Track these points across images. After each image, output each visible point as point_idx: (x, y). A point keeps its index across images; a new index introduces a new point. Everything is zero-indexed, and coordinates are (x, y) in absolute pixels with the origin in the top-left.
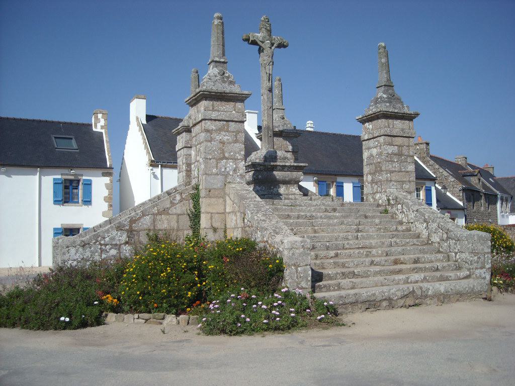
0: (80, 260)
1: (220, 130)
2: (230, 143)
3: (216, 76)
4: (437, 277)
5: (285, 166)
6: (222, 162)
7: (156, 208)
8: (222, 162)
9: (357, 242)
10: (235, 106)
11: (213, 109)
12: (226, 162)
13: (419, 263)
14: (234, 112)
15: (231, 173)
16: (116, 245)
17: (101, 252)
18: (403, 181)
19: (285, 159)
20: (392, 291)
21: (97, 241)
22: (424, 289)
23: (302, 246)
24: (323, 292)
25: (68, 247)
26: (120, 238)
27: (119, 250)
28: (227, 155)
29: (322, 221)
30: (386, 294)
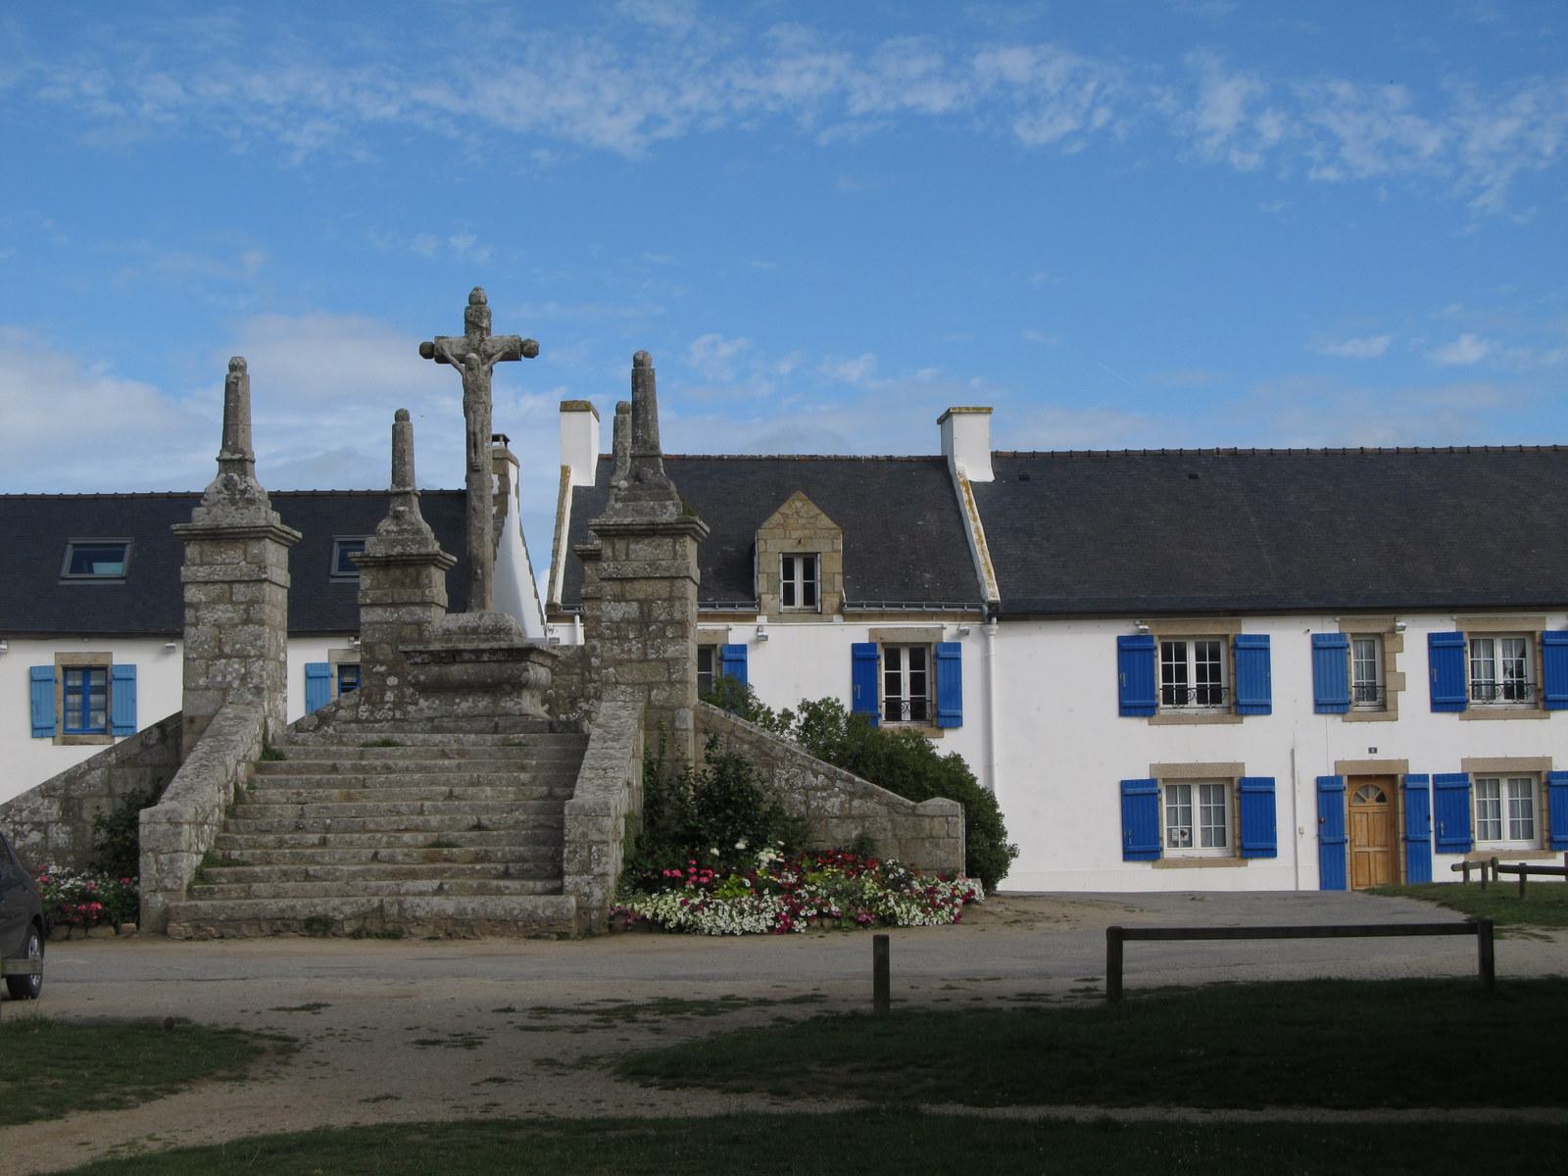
1: (213, 603)
2: (235, 626)
3: (219, 492)
4: (471, 886)
5: (483, 651)
7: (113, 755)
9: (421, 818)
10: (245, 552)
11: (201, 561)
12: (227, 664)
13: (489, 861)
14: (243, 563)
16: (40, 824)
17: (15, 835)
18: (652, 683)
19: (498, 633)
20: (331, 904)
21: (7, 816)
23: (169, 819)
24: (214, 899)
26: (49, 811)
27: (46, 833)
28: (227, 649)
29: (387, 778)
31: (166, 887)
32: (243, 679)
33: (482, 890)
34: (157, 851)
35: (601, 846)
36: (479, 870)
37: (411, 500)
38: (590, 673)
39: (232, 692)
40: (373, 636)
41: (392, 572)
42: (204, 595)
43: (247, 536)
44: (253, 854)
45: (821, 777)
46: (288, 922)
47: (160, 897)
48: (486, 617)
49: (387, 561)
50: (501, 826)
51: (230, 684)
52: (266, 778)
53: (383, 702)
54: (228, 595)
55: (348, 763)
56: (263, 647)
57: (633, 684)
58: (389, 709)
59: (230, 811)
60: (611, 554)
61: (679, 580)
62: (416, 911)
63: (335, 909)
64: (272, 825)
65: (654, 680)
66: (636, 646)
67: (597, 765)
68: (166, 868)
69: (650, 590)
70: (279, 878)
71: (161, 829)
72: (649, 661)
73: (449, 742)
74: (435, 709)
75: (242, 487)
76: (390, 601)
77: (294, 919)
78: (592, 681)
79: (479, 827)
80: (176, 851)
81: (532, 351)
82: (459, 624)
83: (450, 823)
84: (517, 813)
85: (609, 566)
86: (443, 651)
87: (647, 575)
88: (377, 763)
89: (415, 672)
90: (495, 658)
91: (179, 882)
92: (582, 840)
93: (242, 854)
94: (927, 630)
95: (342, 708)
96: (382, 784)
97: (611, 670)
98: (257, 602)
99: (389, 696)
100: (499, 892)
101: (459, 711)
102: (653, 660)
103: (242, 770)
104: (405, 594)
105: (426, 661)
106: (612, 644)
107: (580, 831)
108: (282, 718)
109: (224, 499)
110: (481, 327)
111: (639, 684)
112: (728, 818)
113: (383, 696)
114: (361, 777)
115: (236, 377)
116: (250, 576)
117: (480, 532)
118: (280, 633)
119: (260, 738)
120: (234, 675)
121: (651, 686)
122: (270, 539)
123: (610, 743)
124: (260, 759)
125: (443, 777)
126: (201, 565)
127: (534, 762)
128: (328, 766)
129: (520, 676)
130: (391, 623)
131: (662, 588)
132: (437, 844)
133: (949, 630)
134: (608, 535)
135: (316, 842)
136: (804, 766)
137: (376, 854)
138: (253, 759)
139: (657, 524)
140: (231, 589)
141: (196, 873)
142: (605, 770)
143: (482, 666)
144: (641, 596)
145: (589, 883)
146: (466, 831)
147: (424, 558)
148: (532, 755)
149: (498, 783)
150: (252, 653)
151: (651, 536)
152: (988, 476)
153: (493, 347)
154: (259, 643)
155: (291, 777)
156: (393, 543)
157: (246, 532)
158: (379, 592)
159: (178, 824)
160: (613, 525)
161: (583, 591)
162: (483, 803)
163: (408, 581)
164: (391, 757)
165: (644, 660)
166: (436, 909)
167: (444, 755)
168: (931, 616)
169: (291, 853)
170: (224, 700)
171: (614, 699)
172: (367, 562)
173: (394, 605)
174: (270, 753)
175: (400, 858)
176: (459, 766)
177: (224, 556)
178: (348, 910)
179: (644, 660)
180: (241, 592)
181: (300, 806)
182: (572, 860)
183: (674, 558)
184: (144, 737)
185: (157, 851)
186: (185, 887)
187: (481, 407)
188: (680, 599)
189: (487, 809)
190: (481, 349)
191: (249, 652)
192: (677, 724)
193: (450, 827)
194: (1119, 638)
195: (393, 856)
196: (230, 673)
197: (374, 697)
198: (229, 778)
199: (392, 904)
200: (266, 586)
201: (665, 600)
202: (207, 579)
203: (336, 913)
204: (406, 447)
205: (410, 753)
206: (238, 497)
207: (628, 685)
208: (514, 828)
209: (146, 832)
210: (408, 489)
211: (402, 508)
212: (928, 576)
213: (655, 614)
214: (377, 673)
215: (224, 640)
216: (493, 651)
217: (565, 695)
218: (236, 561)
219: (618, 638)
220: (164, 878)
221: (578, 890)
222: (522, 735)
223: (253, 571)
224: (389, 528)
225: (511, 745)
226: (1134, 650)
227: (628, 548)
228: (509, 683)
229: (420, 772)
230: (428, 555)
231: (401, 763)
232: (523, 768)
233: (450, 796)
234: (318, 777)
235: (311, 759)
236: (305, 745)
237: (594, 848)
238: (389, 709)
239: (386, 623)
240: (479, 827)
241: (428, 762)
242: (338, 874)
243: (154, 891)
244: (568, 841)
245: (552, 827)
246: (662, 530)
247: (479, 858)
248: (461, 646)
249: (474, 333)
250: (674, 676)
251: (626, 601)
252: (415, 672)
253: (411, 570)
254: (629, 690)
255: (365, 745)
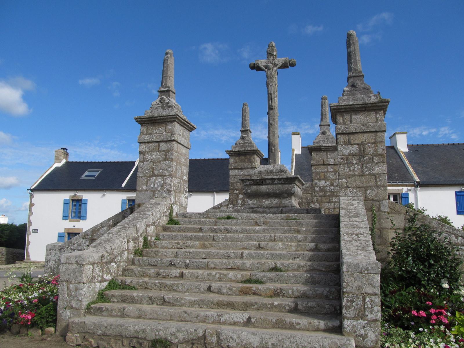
0: (57, 260)
2: (160, 162)
5: (275, 179)
6: (152, 179)
7: (111, 221)
8: (152, 179)
9: (241, 261)
14: (165, 133)
15: (159, 189)
21: (69, 246)
22: (223, 337)
23: (76, 262)
25: (50, 250)
28: (156, 172)
29: (225, 236)
30: (161, 333)
31: (72, 306)
32: (162, 186)
33: (280, 325)
34: (68, 282)
35: (373, 298)
36: (277, 306)
37: (248, 133)
38: (315, 193)
39: (157, 192)
40: (234, 180)
41: (241, 157)
42: (147, 148)
43: (166, 120)
44: (138, 282)
45: (460, 239)
46: (141, 341)
47: (68, 312)
48: (276, 166)
49: (239, 153)
50: (290, 269)
51: (156, 188)
52: (165, 233)
53: (237, 204)
54: (157, 148)
55: (207, 227)
56: (172, 171)
57: (357, 187)
58: (239, 207)
59: (138, 253)
60: (342, 121)
61: (380, 133)
62: (229, 342)
63: (172, 334)
64: (157, 263)
65: (368, 185)
66: (357, 168)
67: (350, 232)
68: (73, 293)
69: (364, 139)
70: (147, 301)
71: (72, 267)
72: (365, 175)
73: (260, 217)
74: (254, 204)
75: (167, 101)
76: (240, 167)
77: (145, 339)
78: (315, 196)
79: (275, 269)
80: (80, 283)
81: (293, 63)
82: (265, 169)
83: (258, 265)
84: (298, 260)
85: (341, 127)
86: (258, 179)
87: (362, 131)
88: (222, 227)
89: (246, 189)
90: (280, 182)
91: (80, 303)
92: (357, 292)
93: (131, 282)
94: (398, 189)
95: (222, 206)
96: (223, 239)
97: (344, 180)
98: (170, 151)
99: (240, 202)
100: (292, 327)
101: (265, 205)
102: (367, 175)
103: (151, 230)
104: (246, 165)
105: (251, 184)
106: (344, 167)
107: (356, 285)
108: (184, 205)
109: (159, 107)
110: (273, 55)
111: (360, 188)
112: (431, 265)
113: (237, 202)
114: (212, 234)
115: (167, 57)
116: (167, 138)
117: (273, 133)
118: (183, 167)
119: (167, 214)
120: (159, 184)
121: (366, 189)
122: (176, 122)
123: (353, 219)
124: (167, 224)
125: (255, 236)
126: (146, 135)
127: (304, 229)
128: (197, 228)
129: (291, 190)
130: (241, 175)
131: (370, 137)
132: (249, 281)
133: (405, 190)
134: (341, 112)
135: (178, 275)
136: (450, 232)
137: (210, 287)
138: (161, 224)
139: (367, 104)
140: (159, 145)
141: (98, 295)
142: (357, 235)
143: (275, 186)
144: (359, 141)
145: (364, 327)
146: (268, 271)
147: (252, 151)
148: (302, 225)
149: (285, 240)
150: (167, 174)
151: (364, 111)
152: (407, 150)
153: (278, 62)
154: (170, 169)
155: (179, 234)
156: (242, 147)
157: (166, 119)
158: (236, 164)
159: (82, 265)
160: (343, 106)
161: (312, 162)
162: (278, 252)
163: (246, 160)
164: (230, 224)
165: (362, 175)
166: (244, 342)
167: (257, 224)
168: (399, 186)
169: (159, 283)
170: (154, 196)
171: (346, 195)
172: (232, 153)
173: (241, 169)
174: (172, 221)
175: (225, 291)
176: (264, 230)
177: (157, 130)
178: (181, 336)
179: (362, 175)
180: (163, 146)
181: (176, 250)
182: (349, 308)
183: (377, 122)
184: (124, 213)
185: (68, 282)
186: (84, 307)
187: (273, 83)
188: (381, 142)
189: (280, 257)
190: (273, 63)
191: (166, 173)
192: (382, 209)
193: (258, 268)
194: (456, 192)
195: (221, 289)
196: (157, 183)
197: (234, 202)
198: (139, 234)
199: (212, 335)
200: (174, 143)
201: (372, 143)
202: (149, 141)
203: (173, 338)
204: (246, 115)
205: (239, 223)
206: (165, 106)
207: (353, 188)
208: (297, 270)
209: (64, 270)
210: (247, 129)
211: (245, 135)
212: (396, 175)
213: (367, 151)
214: (235, 193)
215: (155, 168)
216: (279, 179)
217: (305, 202)
218: (161, 132)
219: (347, 163)
220: (71, 300)
221: (355, 332)
222: (296, 214)
223: (169, 136)
224: (240, 142)
225: (291, 220)
226: (460, 195)
227: (351, 118)
228: (286, 193)
229: (243, 232)
230: (254, 150)
231: (234, 228)
232: (298, 232)
233: (259, 247)
234: (190, 234)
235: (192, 225)
236: (191, 218)
237: (368, 299)
238: (239, 207)
239: (239, 175)
240: (275, 269)
241: (248, 228)
242: (183, 301)
243: (65, 308)
244: (346, 292)
245: (322, 270)
246: (370, 107)
247: (277, 294)
248: (266, 177)
249: (271, 57)
250: (379, 183)
251: (351, 145)
252: (246, 189)
253: (248, 157)
254: (354, 191)
255: (219, 218)
